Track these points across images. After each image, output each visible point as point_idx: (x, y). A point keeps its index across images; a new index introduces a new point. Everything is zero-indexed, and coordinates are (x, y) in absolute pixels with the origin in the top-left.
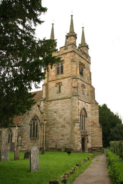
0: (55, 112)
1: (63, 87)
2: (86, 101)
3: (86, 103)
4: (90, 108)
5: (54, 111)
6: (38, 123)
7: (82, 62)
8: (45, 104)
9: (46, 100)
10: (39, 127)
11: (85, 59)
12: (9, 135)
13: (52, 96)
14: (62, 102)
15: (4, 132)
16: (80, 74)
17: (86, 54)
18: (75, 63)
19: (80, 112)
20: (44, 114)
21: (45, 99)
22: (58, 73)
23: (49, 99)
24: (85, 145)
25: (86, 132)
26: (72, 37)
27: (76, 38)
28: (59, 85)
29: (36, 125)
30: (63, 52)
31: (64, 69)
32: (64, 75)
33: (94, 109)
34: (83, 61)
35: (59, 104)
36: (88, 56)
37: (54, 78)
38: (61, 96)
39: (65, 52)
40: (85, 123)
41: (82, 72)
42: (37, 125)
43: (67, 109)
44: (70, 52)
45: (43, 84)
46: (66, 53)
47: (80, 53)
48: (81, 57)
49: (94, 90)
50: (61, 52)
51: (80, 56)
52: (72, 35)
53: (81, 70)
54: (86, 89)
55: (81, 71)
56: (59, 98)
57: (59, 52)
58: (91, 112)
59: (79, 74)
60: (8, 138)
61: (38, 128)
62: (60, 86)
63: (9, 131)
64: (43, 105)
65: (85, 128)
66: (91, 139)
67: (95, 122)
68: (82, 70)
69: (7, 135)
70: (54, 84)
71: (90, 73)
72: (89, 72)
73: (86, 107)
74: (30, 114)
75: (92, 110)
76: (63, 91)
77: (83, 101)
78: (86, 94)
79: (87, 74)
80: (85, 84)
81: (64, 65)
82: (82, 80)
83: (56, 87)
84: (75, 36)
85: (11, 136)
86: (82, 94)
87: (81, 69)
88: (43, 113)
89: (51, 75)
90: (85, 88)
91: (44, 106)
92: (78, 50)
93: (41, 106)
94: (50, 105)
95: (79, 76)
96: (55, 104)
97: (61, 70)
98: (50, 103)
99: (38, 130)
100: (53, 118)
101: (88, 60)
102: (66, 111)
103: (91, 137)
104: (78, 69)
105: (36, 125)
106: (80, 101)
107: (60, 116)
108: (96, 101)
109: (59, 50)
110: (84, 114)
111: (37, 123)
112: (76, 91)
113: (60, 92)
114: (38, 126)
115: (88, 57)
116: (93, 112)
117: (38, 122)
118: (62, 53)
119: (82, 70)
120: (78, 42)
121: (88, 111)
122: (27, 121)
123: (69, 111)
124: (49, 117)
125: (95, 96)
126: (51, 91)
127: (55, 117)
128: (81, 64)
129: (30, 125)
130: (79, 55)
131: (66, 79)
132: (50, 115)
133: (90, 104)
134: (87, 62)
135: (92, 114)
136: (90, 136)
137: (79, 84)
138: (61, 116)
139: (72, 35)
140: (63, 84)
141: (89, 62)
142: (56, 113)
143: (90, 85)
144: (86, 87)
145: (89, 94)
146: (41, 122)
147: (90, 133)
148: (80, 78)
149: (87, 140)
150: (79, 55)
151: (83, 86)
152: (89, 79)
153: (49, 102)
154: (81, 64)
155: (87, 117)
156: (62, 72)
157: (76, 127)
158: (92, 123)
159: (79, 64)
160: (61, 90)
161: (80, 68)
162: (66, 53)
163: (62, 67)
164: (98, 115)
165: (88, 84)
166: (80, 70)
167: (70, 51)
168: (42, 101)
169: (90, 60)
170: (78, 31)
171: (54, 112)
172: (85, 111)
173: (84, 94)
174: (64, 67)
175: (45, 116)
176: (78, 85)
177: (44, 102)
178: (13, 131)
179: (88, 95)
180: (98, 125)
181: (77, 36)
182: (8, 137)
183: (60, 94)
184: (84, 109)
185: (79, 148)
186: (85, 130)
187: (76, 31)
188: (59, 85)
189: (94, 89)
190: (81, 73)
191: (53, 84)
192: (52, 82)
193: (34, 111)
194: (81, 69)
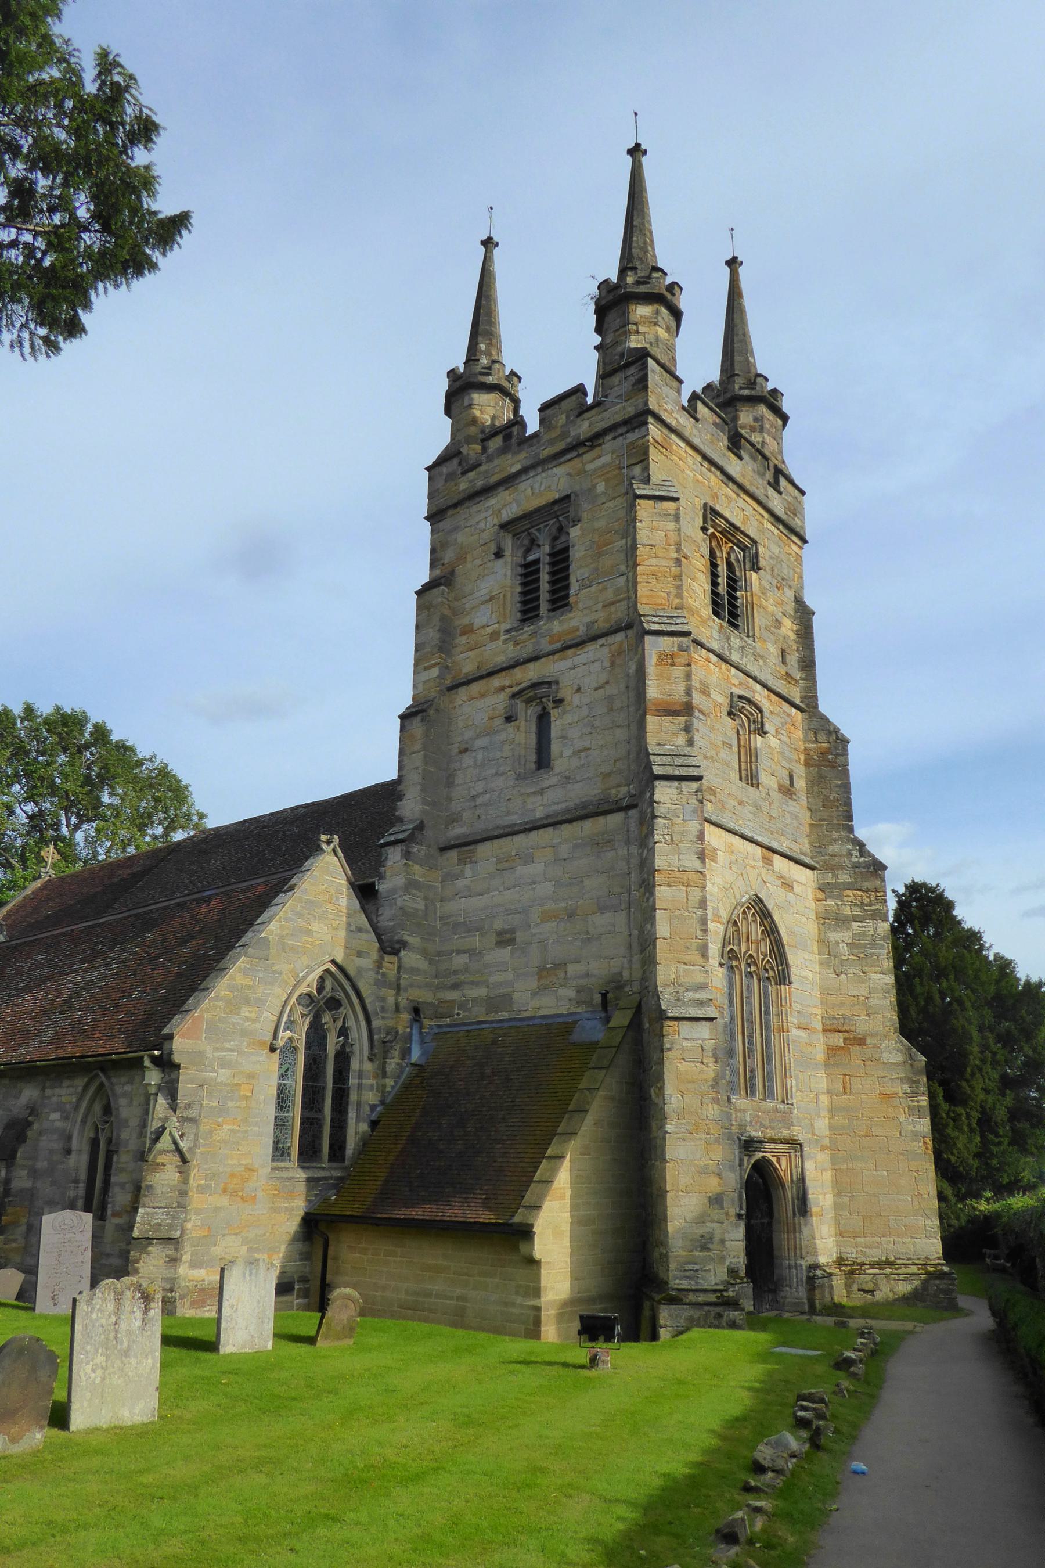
0: (505, 939)
1: (568, 718)
2: (775, 845)
3: (777, 859)
4: (812, 904)
5: (499, 924)
6: (353, 1034)
7: (727, 514)
8: (418, 871)
9: (428, 833)
10: (361, 1075)
11: (759, 493)
12: (95, 1143)
13: (479, 801)
14: (564, 850)
15: (55, 1116)
16: (716, 613)
17: (765, 458)
18: (670, 506)
19: (716, 929)
20: (409, 958)
21: (420, 827)
22: (529, 611)
23: (458, 831)
24: (782, 1239)
25: (786, 1119)
26: (642, 311)
27: (677, 314)
28: (541, 701)
29: (331, 1050)
30: (564, 435)
31: (577, 573)
32: (574, 623)
33: (847, 910)
34: (737, 510)
35: (536, 868)
36: (778, 475)
37: (500, 652)
38: (550, 796)
39: (584, 428)
40: (775, 1039)
41: (733, 598)
42: (343, 1058)
43: (602, 909)
44: (625, 422)
45: (402, 710)
46: (594, 440)
47: (718, 447)
48: (724, 473)
49: (845, 753)
50: (553, 434)
51: (712, 463)
52: (643, 289)
53: (723, 581)
54: (773, 742)
55: (722, 589)
56: (539, 814)
57: (535, 435)
58: (823, 941)
59: (707, 611)
60: (83, 1176)
61: (353, 1081)
62: (543, 721)
63: (97, 1108)
64: (399, 881)
65: (768, 1077)
66: (828, 1175)
67: (862, 1025)
68: (733, 583)
69: (80, 1144)
70: (499, 702)
71: (804, 615)
72: (790, 607)
73: (774, 898)
74: (273, 951)
75: (831, 920)
76: (567, 752)
77: (743, 837)
78: (764, 778)
79: (778, 623)
80: (760, 695)
81: (575, 532)
82: (735, 657)
83: (510, 727)
84: (666, 300)
85: (109, 1155)
86: (734, 775)
87: (723, 570)
88: (404, 944)
89: (468, 630)
90: (762, 732)
91: (411, 885)
92: (691, 411)
93: (382, 887)
94: (461, 883)
95: (709, 628)
96: (506, 864)
97: (552, 583)
98: (462, 861)
99: (353, 1097)
100: (482, 992)
101: (777, 504)
102: (600, 921)
103: (833, 1160)
104: (699, 565)
105: (331, 1050)
106: (714, 837)
107: (542, 971)
108: (861, 845)
109: (533, 425)
110: (760, 954)
111: (343, 1032)
112: (681, 739)
113: (543, 760)
114: (355, 1065)
115: (783, 482)
116: (841, 936)
117: (351, 1023)
118: (561, 446)
119: (733, 583)
120: (698, 360)
121: (792, 933)
122: (245, 1011)
123: (621, 919)
124: (455, 986)
125: (848, 803)
126: (467, 760)
127: (496, 978)
128: (719, 529)
129: (273, 1049)
130: (705, 457)
131: (592, 651)
132: (459, 961)
133: (809, 872)
134: (776, 519)
135: (827, 949)
136: (823, 1157)
137: (705, 692)
138: (549, 972)
139: (631, 295)
140: (566, 693)
141: (796, 523)
142: (511, 942)
143: (809, 705)
144: (768, 727)
145: (800, 784)
146: (376, 1023)
147: (822, 1125)
148: (715, 646)
149: (790, 1192)
150: (705, 457)
151: (740, 707)
152: (793, 659)
153: (453, 854)
154: (719, 529)
155: (783, 978)
156: (560, 601)
157: (683, 1066)
158: (838, 1040)
159: (704, 529)
160: (555, 747)
161: (714, 565)
162: (594, 440)
163: (561, 559)
164: (888, 964)
165: (792, 704)
166: (714, 584)
167: (619, 418)
168: (390, 850)
169: (796, 510)
170: (682, 253)
171: (493, 938)
172: (771, 931)
173: (751, 779)
174: (577, 554)
175: (414, 971)
176: (697, 698)
177: (407, 855)
178: (123, 1101)
179: (788, 790)
180: (893, 1049)
181: (684, 302)
182: (85, 1158)
183: (549, 779)
184: (760, 910)
185: (715, 1276)
186: (769, 1093)
187: (672, 253)
188: (533, 711)
189: (841, 743)
190: (728, 606)
191: (490, 701)
192: (475, 688)
193: (315, 927)
194: (723, 570)
